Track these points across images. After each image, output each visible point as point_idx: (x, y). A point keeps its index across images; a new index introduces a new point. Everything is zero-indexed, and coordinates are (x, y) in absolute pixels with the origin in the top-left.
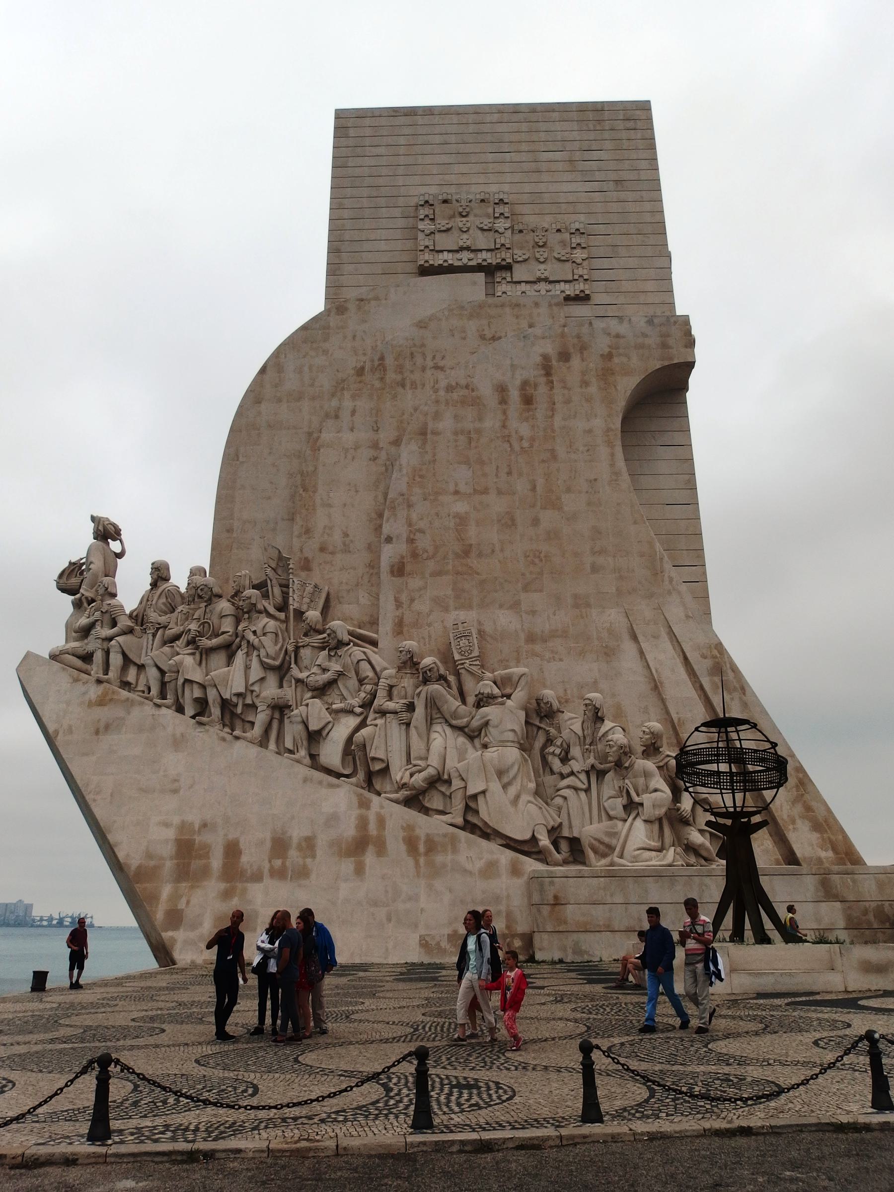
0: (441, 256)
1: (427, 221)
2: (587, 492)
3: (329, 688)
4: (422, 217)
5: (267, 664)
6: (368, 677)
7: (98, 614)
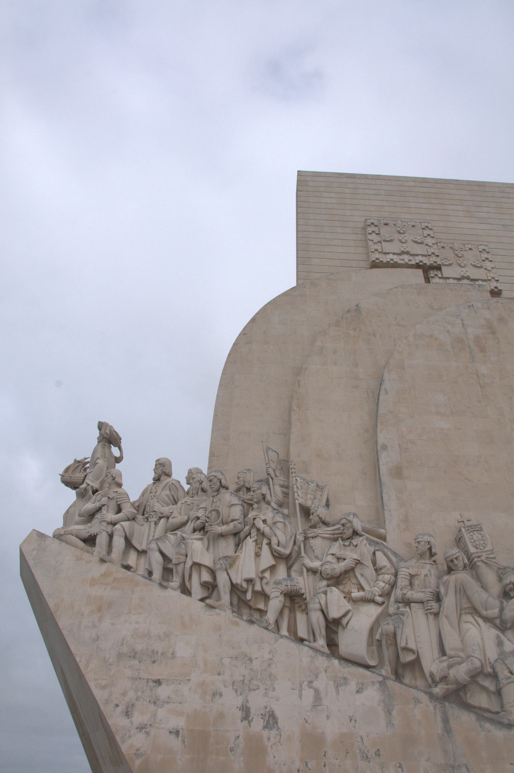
0: (388, 256)
1: (374, 235)
4: (370, 232)
6: (385, 566)
7: (104, 500)
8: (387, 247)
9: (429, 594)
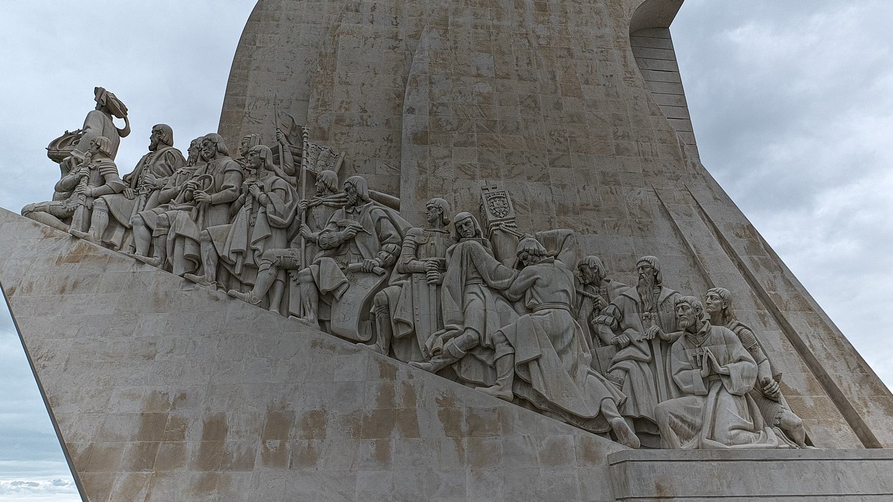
2: (604, 85)
3: (343, 248)
6: (391, 235)
7: (84, 170)
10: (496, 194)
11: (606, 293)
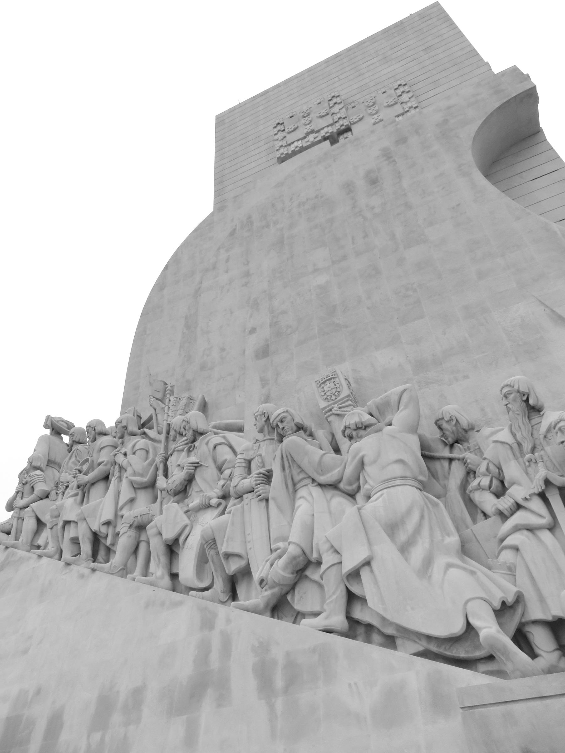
5: (136, 482)
6: (226, 460)
8: (290, 138)
9: (256, 477)
10: (325, 377)
11: (477, 447)
